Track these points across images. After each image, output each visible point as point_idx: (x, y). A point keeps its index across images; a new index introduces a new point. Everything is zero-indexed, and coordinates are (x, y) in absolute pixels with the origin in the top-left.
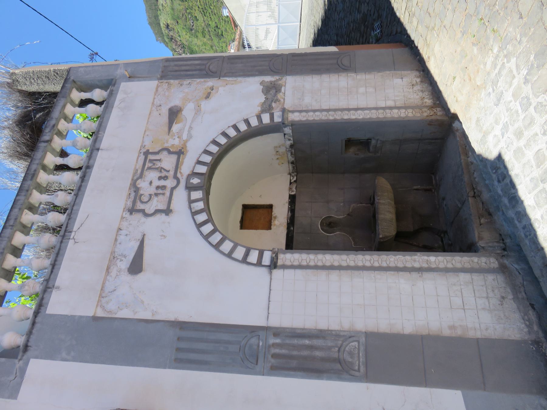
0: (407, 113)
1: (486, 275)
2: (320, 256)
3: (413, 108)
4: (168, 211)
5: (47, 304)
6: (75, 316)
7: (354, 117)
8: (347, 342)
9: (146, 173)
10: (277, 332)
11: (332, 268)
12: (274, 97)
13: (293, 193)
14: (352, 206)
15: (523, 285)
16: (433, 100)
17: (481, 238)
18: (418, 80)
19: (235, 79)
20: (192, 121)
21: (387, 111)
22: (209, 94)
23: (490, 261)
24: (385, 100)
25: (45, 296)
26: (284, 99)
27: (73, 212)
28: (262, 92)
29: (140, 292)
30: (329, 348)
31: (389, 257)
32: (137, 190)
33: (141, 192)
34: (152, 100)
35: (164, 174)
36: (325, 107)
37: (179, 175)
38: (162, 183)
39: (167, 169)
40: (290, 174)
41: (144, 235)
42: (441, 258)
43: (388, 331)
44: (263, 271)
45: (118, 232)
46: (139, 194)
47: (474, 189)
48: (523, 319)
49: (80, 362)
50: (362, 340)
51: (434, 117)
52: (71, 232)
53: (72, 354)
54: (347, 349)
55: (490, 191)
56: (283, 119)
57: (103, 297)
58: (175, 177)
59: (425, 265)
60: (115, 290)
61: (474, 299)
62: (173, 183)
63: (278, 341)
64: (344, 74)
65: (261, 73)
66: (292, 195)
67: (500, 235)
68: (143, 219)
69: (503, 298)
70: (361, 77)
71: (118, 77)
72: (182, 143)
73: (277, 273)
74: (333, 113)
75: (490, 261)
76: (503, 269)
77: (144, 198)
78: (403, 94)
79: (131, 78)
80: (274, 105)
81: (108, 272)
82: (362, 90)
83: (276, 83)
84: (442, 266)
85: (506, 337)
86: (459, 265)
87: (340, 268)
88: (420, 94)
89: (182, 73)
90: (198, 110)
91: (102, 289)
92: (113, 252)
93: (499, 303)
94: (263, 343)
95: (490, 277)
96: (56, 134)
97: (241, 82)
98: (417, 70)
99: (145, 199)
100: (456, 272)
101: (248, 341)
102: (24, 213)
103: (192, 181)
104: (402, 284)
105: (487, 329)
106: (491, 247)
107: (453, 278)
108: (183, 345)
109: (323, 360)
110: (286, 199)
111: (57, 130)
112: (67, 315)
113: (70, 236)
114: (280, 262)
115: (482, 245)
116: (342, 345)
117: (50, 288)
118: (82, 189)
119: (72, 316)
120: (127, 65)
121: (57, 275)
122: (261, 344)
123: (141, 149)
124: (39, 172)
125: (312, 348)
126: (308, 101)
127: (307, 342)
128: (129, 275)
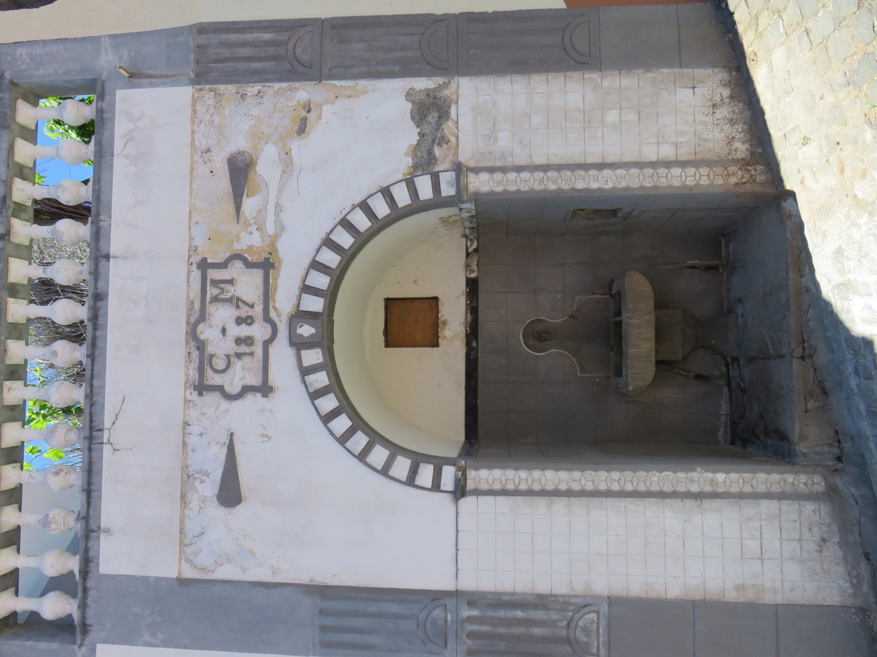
0: (697, 175)
1: (802, 503)
2: (536, 474)
3: (710, 163)
4: (265, 389)
5: (98, 557)
6: (149, 577)
7: (595, 186)
8: (581, 614)
9: (211, 309)
10: (473, 599)
11: (556, 493)
12: (437, 129)
13: (473, 275)
14: (577, 298)
15: (859, 523)
16: (751, 145)
17: (803, 438)
18: (726, 92)
19: (352, 83)
20: (280, 190)
21: (662, 171)
22: (304, 120)
23: (813, 481)
24: (658, 143)
25: (89, 545)
26: (457, 138)
27: (94, 391)
28: (412, 117)
29: (245, 536)
30: (553, 623)
31: (650, 474)
32: (201, 346)
33: (210, 349)
34: (189, 141)
35: (244, 311)
36: (539, 160)
37: (273, 314)
38: (244, 331)
39: (250, 302)
40: (465, 236)
41: (232, 434)
42: (734, 476)
43: (643, 595)
44: (442, 502)
45: (184, 428)
46: (207, 354)
47: (804, 342)
48: (850, 575)
49: (176, 647)
50: (604, 609)
51: (748, 188)
52: (101, 430)
53: (160, 636)
54: (580, 623)
55: (832, 351)
56: (458, 191)
57: (186, 546)
58: (267, 319)
59: (708, 489)
60: (202, 534)
61: (778, 543)
62: (267, 332)
63: (475, 613)
64: (577, 75)
65: (406, 70)
66: (471, 279)
67: (837, 432)
68: (225, 404)
69: (824, 540)
70: (612, 81)
71: (105, 74)
72: (268, 241)
73: (467, 503)
74: (556, 174)
75: (813, 481)
76: (831, 495)
77: (218, 361)
78: (693, 129)
79: (135, 77)
80: (437, 151)
81: (185, 503)
82: (612, 116)
83: (438, 94)
84: (734, 489)
85: (819, 601)
86: (762, 489)
87: (569, 493)
88: (727, 127)
89: (241, 66)
90: (287, 163)
91: (181, 532)
92: (185, 467)
93: (817, 548)
94: (452, 617)
95: (809, 507)
96: (14, 215)
97: (365, 92)
98: (725, 67)
99: (220, 364)
100: (757, 499)
101: (429, 614)
102: (5, 389)
103: (300, 331)
104: (669, 518)
105: (792, 590)
106: (817, 453)
107: (749, 509)
108: (330, 621)
109: (544, 640)
110: (462, 286)
111: (12, 205)
112: (134, 576)
113: (102, 437)
114: (470, 485)
115: (804, 451)
116: (572, 618)
117: (94, 531)
118: (99, 343)
119: (143, 577)
120: (118, 39)
121: (99, 509)
122: (449, 618)
123: (190, 256)
124: (6, 303)
125: (525, 622)
126: (507, 144)
127: (520, 614)
128: (222, 508)
